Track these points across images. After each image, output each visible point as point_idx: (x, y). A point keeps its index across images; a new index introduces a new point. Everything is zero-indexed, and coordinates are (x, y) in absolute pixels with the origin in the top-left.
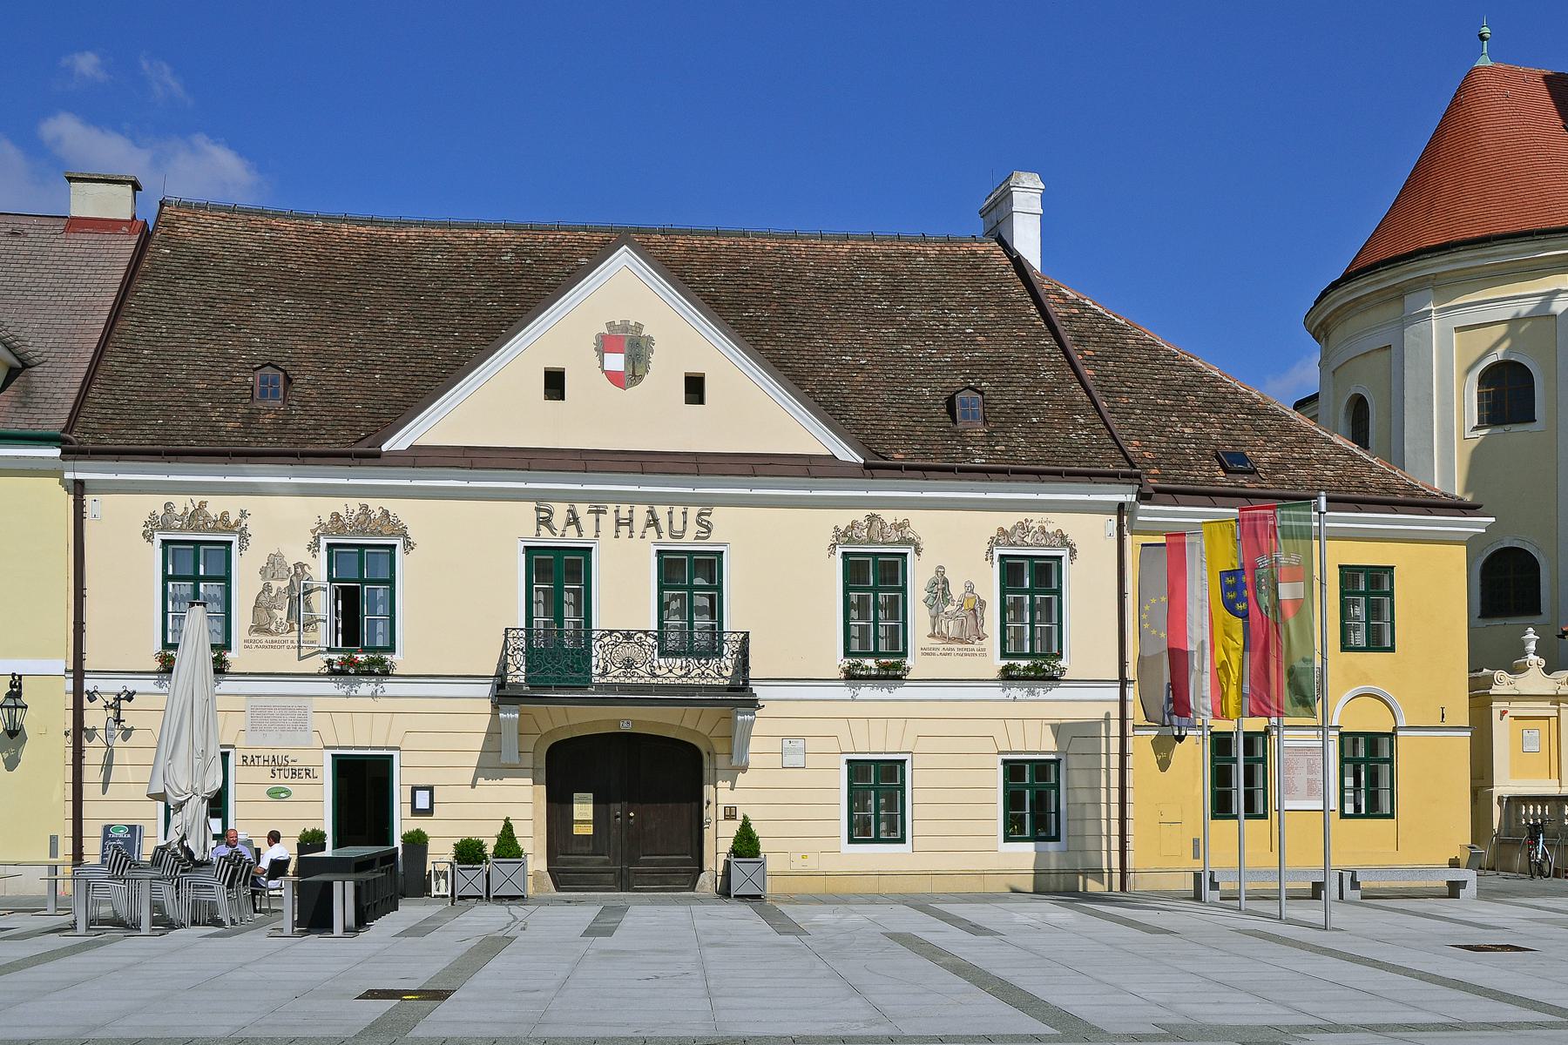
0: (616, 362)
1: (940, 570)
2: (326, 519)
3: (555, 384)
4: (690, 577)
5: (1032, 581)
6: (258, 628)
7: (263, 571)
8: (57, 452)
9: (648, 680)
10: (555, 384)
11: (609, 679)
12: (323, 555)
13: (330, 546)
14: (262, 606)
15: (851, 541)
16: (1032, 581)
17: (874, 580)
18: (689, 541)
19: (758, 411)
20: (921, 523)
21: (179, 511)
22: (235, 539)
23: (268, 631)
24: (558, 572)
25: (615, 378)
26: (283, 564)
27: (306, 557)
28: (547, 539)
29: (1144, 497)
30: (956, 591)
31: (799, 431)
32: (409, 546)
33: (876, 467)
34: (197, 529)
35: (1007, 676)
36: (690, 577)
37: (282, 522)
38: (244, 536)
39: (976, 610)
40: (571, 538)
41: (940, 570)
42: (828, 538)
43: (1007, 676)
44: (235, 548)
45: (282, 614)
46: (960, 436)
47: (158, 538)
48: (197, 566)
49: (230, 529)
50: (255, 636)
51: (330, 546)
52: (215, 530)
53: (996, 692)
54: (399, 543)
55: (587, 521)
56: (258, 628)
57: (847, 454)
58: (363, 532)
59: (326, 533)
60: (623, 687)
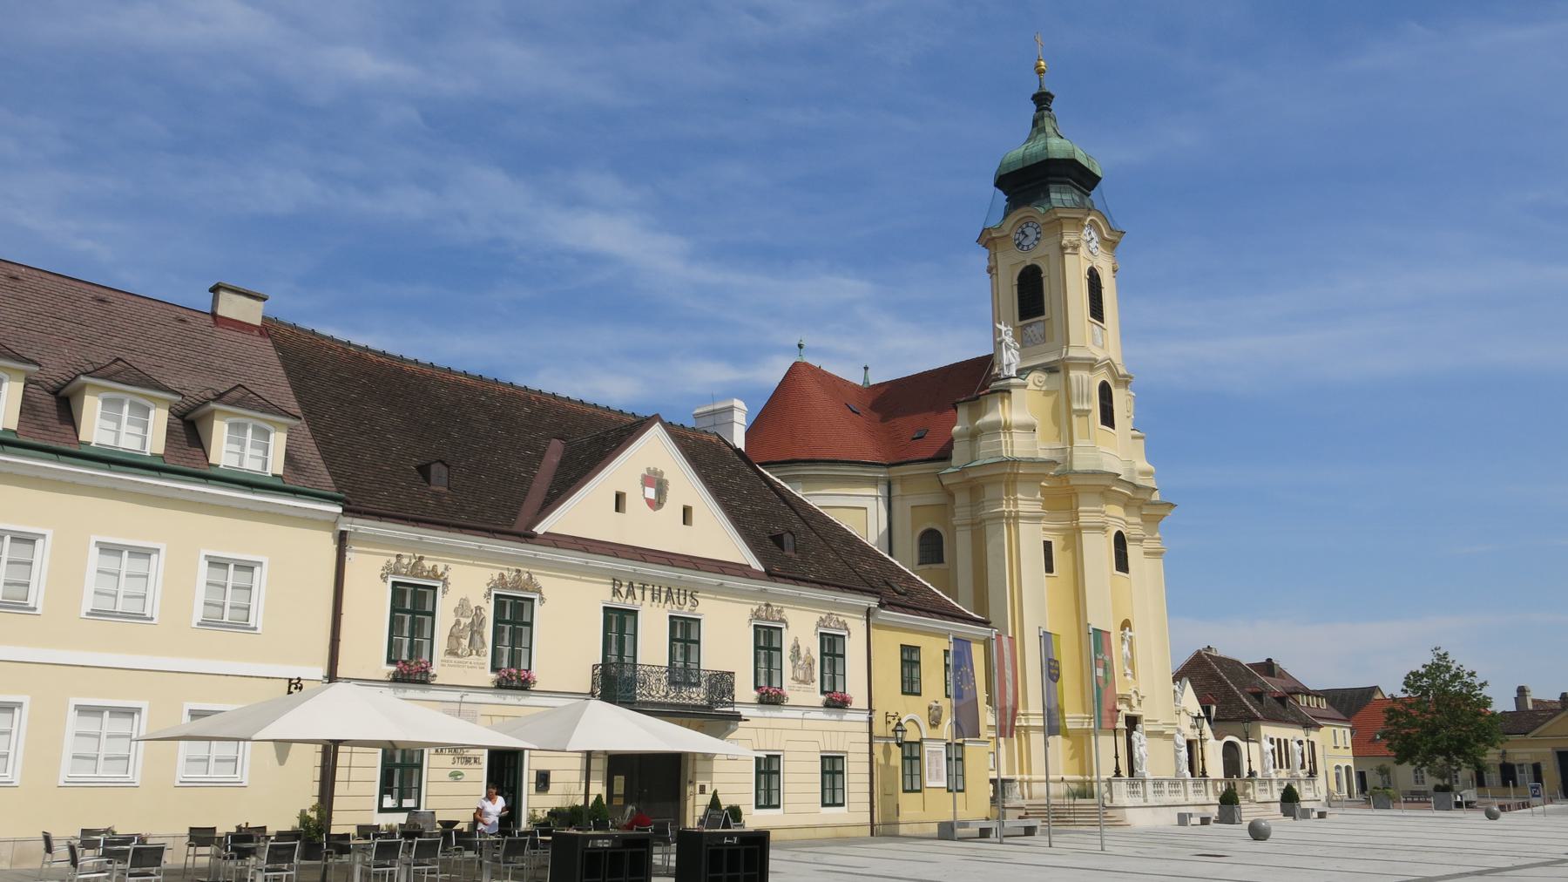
0: (651, 493)
1: (796, 640)
2: (496, 577)
3: (620, 500)
4: (684, 633)
5: (832, 647)
6: (452, 652)
7: (456, 610)
8: (339, 510)
9: (687, 701)
10: (620, 500)
11: (669, 700)
12: (492, 602)
13: (497, 596)
14: (454, 636)
15: (758, 618)
16: (832, 647)
17: (767, 641)
18: (685, 611)
19: (716, 536)
20: (790, 614)
21: (405, 561)
22: (439, 585)
23: (456, 654)
24: (619, 623)
25: (650, 502)
26: (468, 606)
27: (482, 602)
28: (618, 603)
29: (881, 606)
30: (803, 653)
31: (736, 550)
32: (542, 600)
33: (770, 575)
34: (415, 576)
35: (827, 705)
36: (684, 633)
37: (467, 578)
38: (445, 582)
39: (810, 665)
40: (628, 604)
41: (796, 640)
42: (748, 615)
43: (827, 705)
44: (439, 591)
45: (465, 642)
46: (790, 558)
47: (391, 579)
48: (412, 606)
49: (437, 577)
50: (448, 658)
51: (497, 596)
52: (427, 577)
53: (820, 715)
54: (536, 597)
55: (638, 592)
56: (452, 652)
57: (757, 565)
58: (517, 588)
59: (496, 586)
60: (677, 705)
